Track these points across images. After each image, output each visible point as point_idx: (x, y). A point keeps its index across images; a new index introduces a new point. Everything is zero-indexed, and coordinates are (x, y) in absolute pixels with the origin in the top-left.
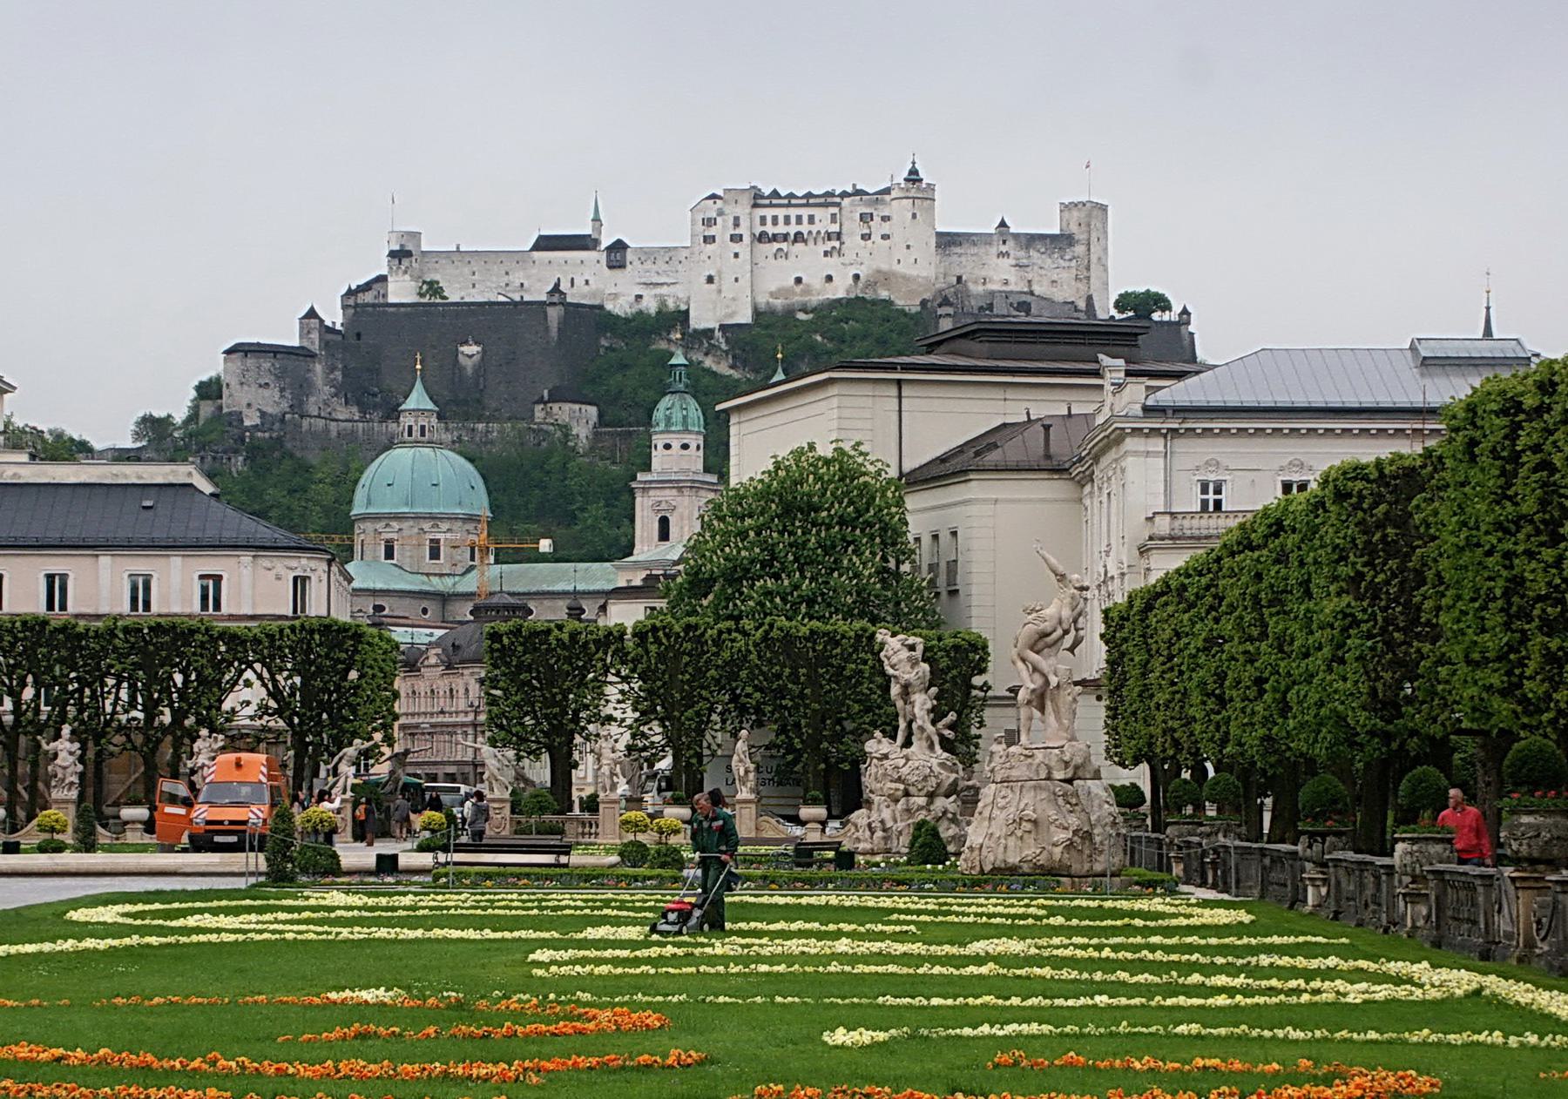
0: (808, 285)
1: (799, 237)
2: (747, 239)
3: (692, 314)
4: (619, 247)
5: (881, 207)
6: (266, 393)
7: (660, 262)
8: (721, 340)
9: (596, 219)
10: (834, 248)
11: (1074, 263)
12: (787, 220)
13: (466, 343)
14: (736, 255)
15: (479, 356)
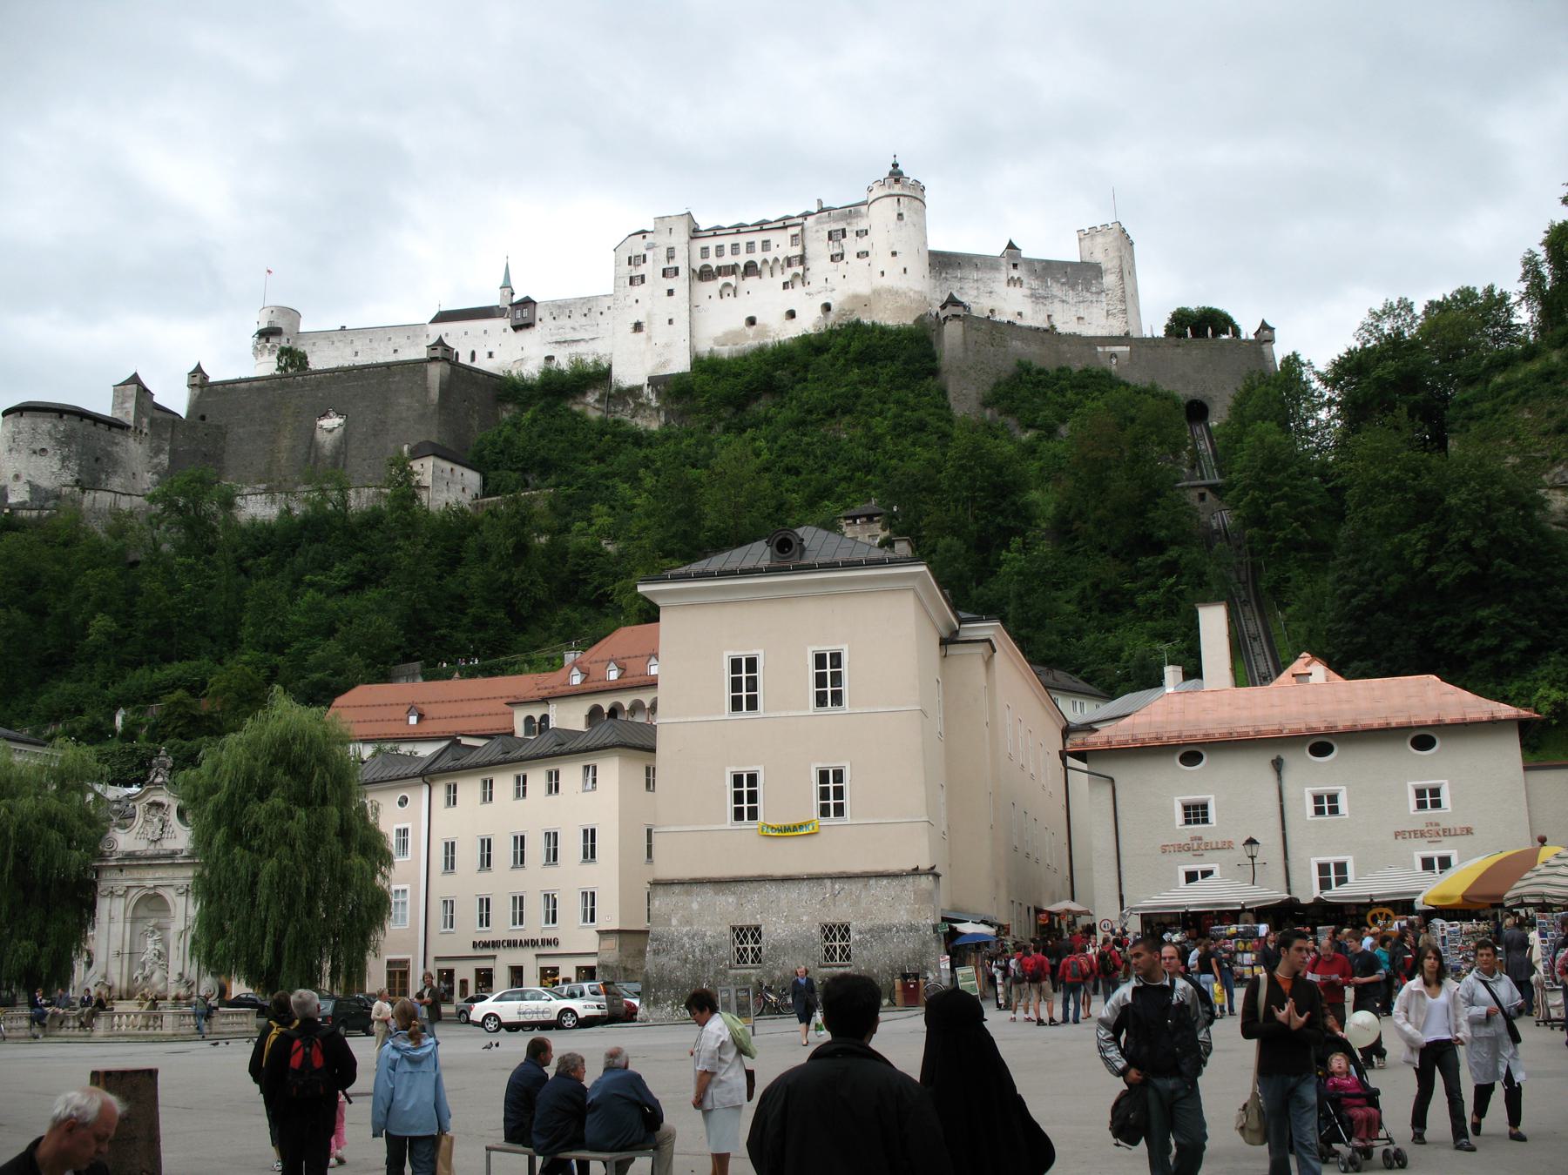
0: (765, 326)
1: (751, 269)
2: (684, 272)
3: (616, 372)
4: (528, 302)
5: (855, 221)
6: (43, 461)
7: (577, 316)
8: (652, 396)
9: (506, 285)
10: (796, 275)
11: (1103, 297)
12: (735, 248)
13: (325, 415)
14: (670, 292)
15: (341, 429)
